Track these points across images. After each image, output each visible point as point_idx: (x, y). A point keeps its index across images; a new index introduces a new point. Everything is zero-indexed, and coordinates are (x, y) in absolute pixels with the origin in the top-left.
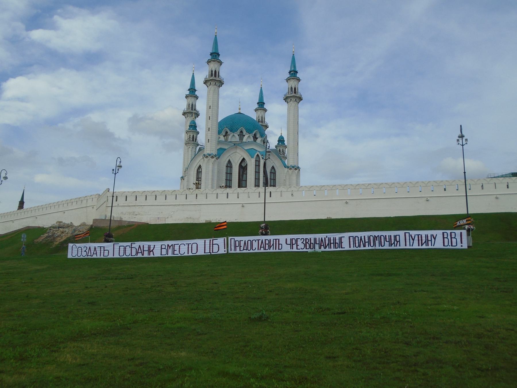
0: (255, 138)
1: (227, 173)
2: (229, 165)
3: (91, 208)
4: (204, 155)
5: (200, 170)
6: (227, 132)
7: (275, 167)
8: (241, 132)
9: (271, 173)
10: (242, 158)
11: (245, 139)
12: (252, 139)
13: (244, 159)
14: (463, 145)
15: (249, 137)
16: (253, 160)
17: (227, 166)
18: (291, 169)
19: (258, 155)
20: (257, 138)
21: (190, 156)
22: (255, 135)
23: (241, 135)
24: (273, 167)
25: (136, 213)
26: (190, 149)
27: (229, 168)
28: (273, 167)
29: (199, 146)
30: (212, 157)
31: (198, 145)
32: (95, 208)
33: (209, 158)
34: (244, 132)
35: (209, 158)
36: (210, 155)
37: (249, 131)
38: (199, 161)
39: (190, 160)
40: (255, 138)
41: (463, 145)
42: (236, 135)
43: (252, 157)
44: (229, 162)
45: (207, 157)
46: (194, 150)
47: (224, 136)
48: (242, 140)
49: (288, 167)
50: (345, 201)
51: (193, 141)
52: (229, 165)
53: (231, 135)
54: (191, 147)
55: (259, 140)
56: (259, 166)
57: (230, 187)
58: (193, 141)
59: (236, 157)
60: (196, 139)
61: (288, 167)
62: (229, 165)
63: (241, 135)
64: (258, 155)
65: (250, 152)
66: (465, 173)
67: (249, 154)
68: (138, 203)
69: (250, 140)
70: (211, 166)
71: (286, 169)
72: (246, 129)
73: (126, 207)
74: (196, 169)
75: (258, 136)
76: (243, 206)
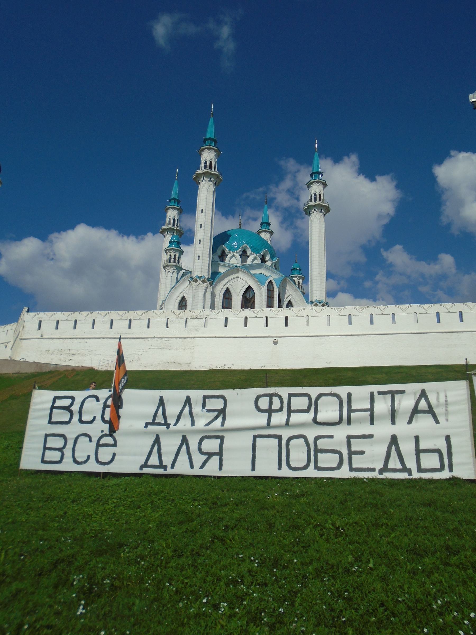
0: (263, 260)
2: (227, 296)
3: (3, 346)
4: (192, 278)
5: (184, 304)
8: (244, 252)
11: (249, 261)
12: (258, 261)
13: (249, 288)
15: (255, 259)
16: (264, 289)
18: (316, 305)
19: (270, 282)
20: (266, 262)
21: (169, 283)
23: (244, 255)
25: (72, 352)
26: (170, 274)
29: (183, 271)
30: (204, 282)
31: (181, 269)
32: (10, 345)
33: (200, 282)
34: (249, 252)
35: (200, 282)
36: (200, 278)
37: (255, 250)
38: (184, 289)
39: (169, 289)
40: (263, 260)
42: (238, 255)
43: (263, 284)
45: (196, 281)
46: (175, 275)
47: (219, 257)
48: (245, 262)
49: (312, 303)
51: (175, 262)
52: (227, 295)
53: (230, 255)
54: (171, 271)
55: (269, 263)
56: (272, 298)
57: (252, 307)
58: (175, 262)
59: (238, 284)
60: (179, 261)
61: (312, 303)
62: (227, 295)
63: (244, 255)
64: (270, 282)
65: (259, 279)
67: (257, 279)
68: (77, 332)
69: (256, 262)
70: (201, 294)
71: (309, 305)
72: (251, 248)
73: (56, 340)
74: (178, 301)
75: (267, 258)
76: (275, 343)
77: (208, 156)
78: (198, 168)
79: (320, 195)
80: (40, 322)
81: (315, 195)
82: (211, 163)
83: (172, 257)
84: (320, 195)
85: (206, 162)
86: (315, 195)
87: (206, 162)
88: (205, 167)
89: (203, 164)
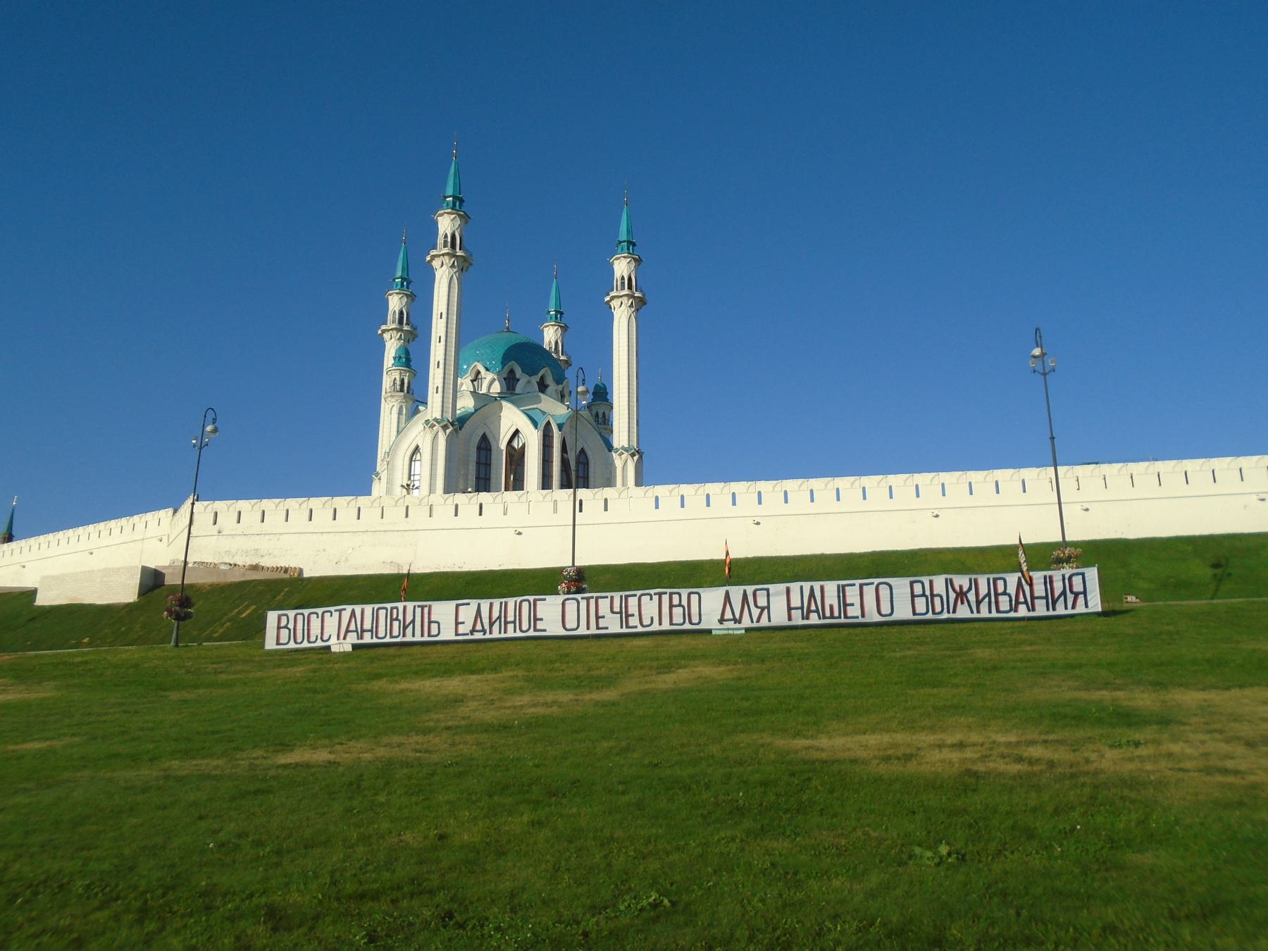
1: (478, 463)
2: (483, 445)
6: (479, 372)
7: (587, 450)
9: (578, 463)
10: (513, 430)
13: (517, 432)
14: (1045, 374)
15: (529, 382)
17: (479, 448)
19: (548, 423)
22: (542, 378)
24: (582, 451)
27: (483, 452)
28: (582, 451)
34: (519, 372)
37: (530, 372)
41: (1045, 374)
44: (484, 438)
50: (750, 521)
66: (1052, 438)
75: (549, 380)
77: (446, 224)
78: (435, 247)
79: (630, 279)
80: (216, 514)
81: (623, 278)
82: (453, 237)
83: (398, 382)
84: (630, 279)
85: (446, 236)
86: (623, 278)
87: (446, 236)
88: (445, 246)
89: (440, 240)
